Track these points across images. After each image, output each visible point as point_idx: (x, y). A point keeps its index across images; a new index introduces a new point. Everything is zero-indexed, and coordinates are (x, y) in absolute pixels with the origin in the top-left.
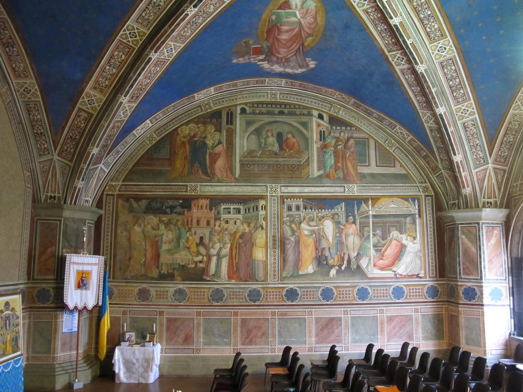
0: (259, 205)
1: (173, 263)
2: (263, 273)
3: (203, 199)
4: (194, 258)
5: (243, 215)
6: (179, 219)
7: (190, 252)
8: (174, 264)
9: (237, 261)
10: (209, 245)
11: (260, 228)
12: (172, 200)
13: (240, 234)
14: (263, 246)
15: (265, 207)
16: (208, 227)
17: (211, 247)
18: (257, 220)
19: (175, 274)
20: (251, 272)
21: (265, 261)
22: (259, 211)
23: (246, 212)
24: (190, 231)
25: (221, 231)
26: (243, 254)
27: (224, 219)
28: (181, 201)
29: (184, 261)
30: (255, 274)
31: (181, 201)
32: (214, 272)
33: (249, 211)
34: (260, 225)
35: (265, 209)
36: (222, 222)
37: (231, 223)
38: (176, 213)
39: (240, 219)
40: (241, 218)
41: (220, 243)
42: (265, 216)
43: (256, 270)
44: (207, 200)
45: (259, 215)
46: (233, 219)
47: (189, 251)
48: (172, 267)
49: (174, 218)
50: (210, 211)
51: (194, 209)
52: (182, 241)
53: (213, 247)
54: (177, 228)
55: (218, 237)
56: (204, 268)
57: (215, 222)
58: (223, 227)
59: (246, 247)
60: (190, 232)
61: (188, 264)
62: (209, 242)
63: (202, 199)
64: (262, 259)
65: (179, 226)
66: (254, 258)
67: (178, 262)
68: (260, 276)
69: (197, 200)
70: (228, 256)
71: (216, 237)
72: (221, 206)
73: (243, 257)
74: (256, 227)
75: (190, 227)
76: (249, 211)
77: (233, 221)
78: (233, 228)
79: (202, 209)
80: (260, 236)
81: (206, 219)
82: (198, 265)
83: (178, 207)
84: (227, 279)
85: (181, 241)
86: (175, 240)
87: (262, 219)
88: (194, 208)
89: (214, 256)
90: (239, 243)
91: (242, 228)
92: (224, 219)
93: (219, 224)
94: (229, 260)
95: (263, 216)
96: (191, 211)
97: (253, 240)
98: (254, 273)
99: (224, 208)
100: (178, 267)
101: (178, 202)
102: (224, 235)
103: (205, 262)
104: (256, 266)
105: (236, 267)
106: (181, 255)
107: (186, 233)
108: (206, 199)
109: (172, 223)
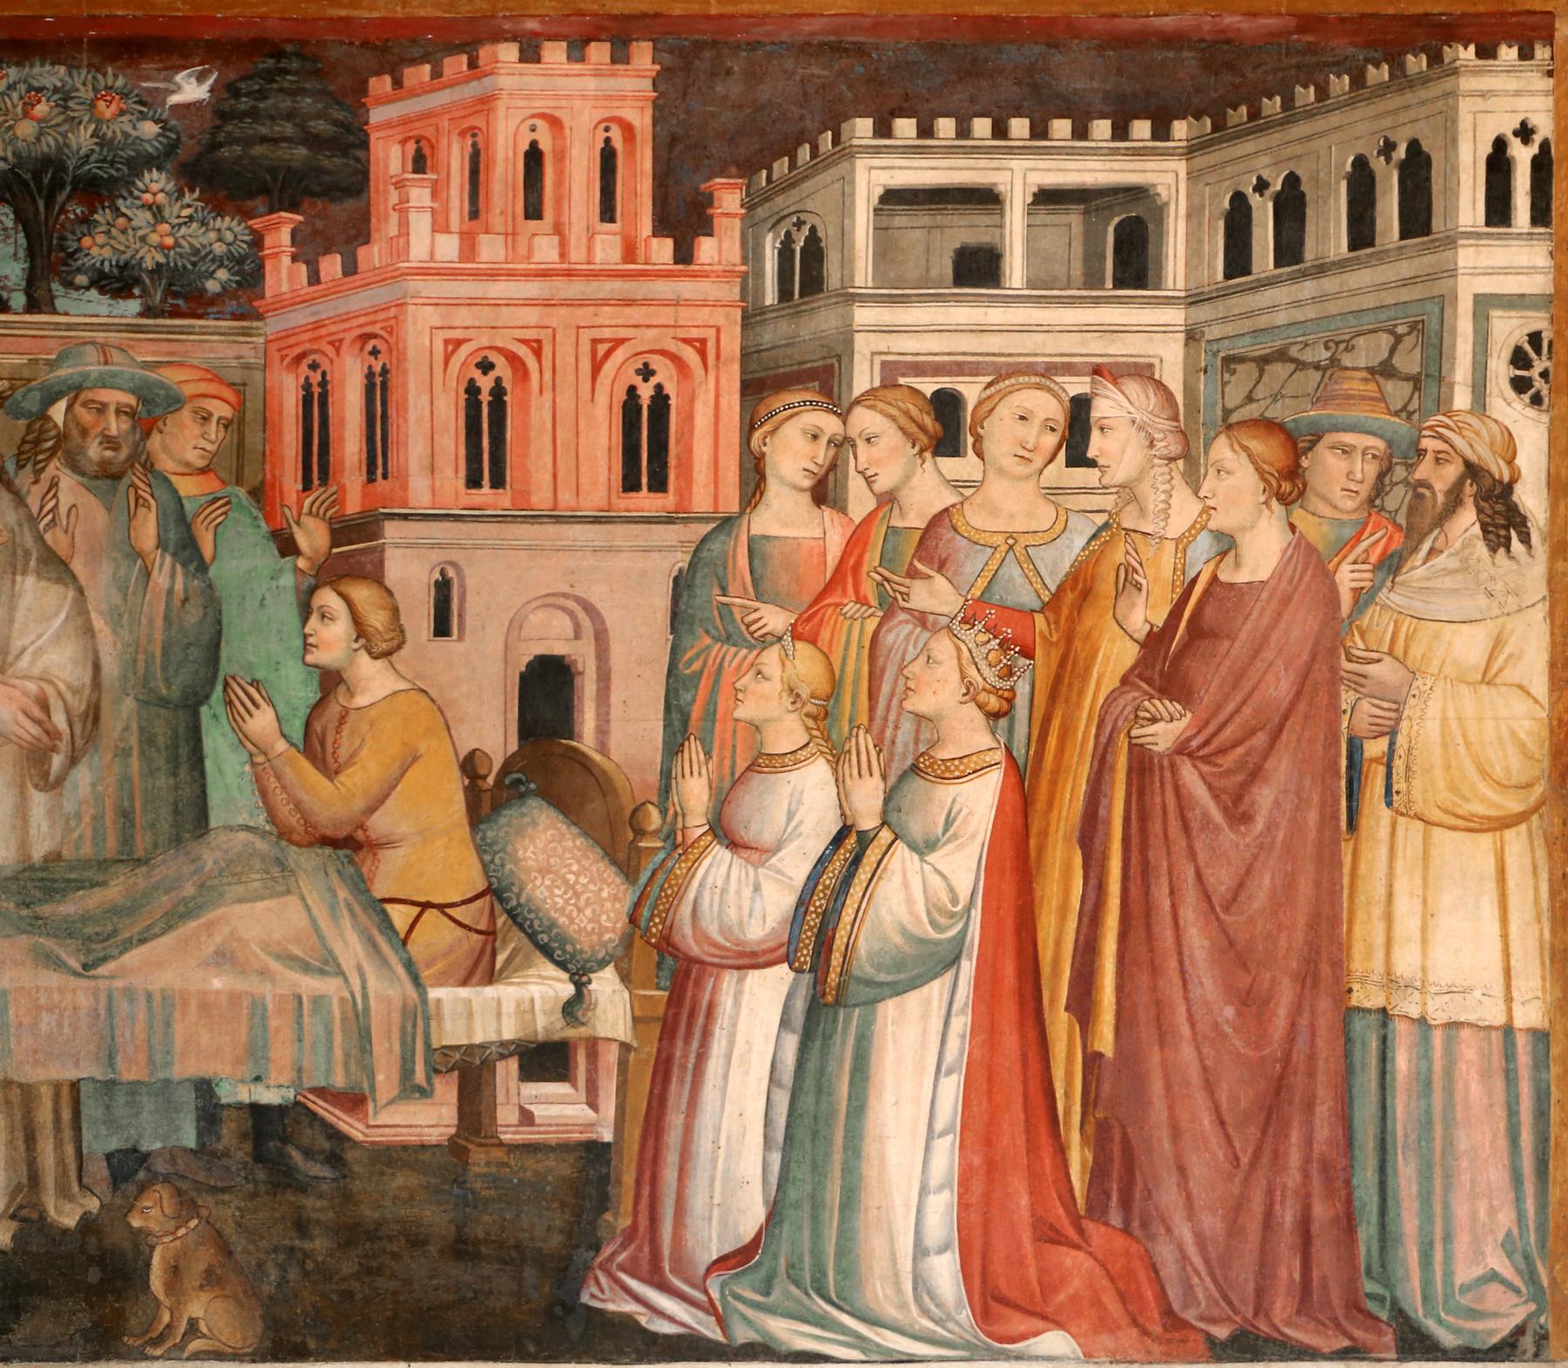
0: (1452, 142)
1: (110, 1085)
2: (1506, 1218)
3: (555, 53)
4: (434, 993)
5: (1194, 299)
6: (171, 376)
7: (379, 907)
8: (134, 1088)
9: (1105, 1041)
10: (666, 775)
11: (1467, 520)
12: (51, 75)
13: (1145, 614)
14: (1514, 805)
15: (1542, 165)
16: (646, 501)
17: (697, 823)
18: (1416, 381)
19: (141, 1243)
20: (1321, 1211)
21: (1540, 1037)
22: (1451, 241)
23: (1238, 259)
24: (376, 576)
25: (846, 572)
26: (1197, 940)
27: (892, 371)
28: (191, 89)
29: (282, 1052)
30: (1386, 1237)
31: (191, 89)
32: (752, 1216)
33: (1289, 250)
34: (1472, 470)
35: (1541, 215)
36: (865, 420)
37: (1002, 432)
38: (117, 282)
39: (1143, 372)
40: (1171, 359)
41: (837, 758)
42: (1539, 321)
43: (1406, 1171)
44: (620, 56)
45: (1444, 302)
46: (1046, 372)
47: (361, 886)
48: (100, 1142)
49: (91, 365)
50: (663, 250)
51: (420, 224)
52: (242, 738)
53: (723, 831)
54: (147, 530)
55: (806, 664)
56: (595, 1152)
57: (749, 427)
58: (888, 500)
59: (1238, 812)
60: (362, 593)
61: (354, 1101)
62: (674, 747)
63: (530, 55)
64: (1494, 1014)
65: (188, 487)
66: (1366, 996)
67: (186, 1068)
68: (1465, 1273)
69: (456, 64)
70: (968, 968)
71: (771, 657)
72: (845, 152)
73: (1207, 985)
74: (1397, 498)
75: (353, 506)
76: (1289, 250)
77: (1047, 407)
78: (1045, 517)
79: (533, 211)
80: (1469, 646)
81: (618, 372)
82: (506, 1115)
83: (157, 183)
84: (965, 1315)
85: (217, 740)
86: (122, 714)
87: (1500, 369)
88: (420, 195)
89: (752, 960)
90: (1142, 763)
91: (1184, 511)
92: (892, 371)
93: (823, 454)
94: (985, 1028)
95: (1509, 330)
96: (372, 255)
97: (1356, 710)
98: (1367, 1232)
99: (894, 198)
100: (189, 1137)
101: (148, 104)
102: (900, 633)
103: (610, 1056)
104: (1401, 1106)
105: (1100, 1137)
106: (224, 958)
107: (305, 611)
108: (599, 52)
109: (66, 447)
